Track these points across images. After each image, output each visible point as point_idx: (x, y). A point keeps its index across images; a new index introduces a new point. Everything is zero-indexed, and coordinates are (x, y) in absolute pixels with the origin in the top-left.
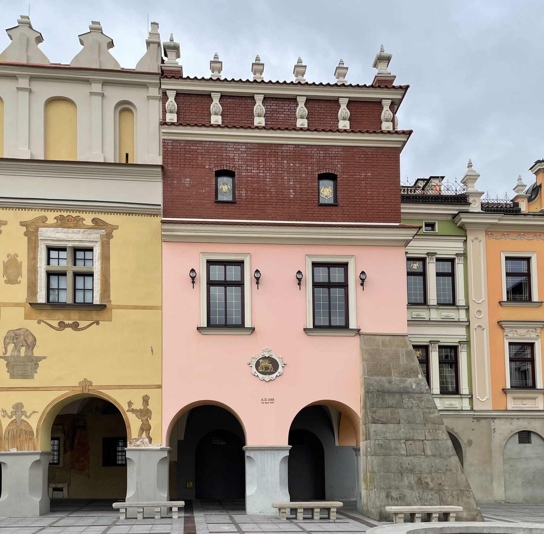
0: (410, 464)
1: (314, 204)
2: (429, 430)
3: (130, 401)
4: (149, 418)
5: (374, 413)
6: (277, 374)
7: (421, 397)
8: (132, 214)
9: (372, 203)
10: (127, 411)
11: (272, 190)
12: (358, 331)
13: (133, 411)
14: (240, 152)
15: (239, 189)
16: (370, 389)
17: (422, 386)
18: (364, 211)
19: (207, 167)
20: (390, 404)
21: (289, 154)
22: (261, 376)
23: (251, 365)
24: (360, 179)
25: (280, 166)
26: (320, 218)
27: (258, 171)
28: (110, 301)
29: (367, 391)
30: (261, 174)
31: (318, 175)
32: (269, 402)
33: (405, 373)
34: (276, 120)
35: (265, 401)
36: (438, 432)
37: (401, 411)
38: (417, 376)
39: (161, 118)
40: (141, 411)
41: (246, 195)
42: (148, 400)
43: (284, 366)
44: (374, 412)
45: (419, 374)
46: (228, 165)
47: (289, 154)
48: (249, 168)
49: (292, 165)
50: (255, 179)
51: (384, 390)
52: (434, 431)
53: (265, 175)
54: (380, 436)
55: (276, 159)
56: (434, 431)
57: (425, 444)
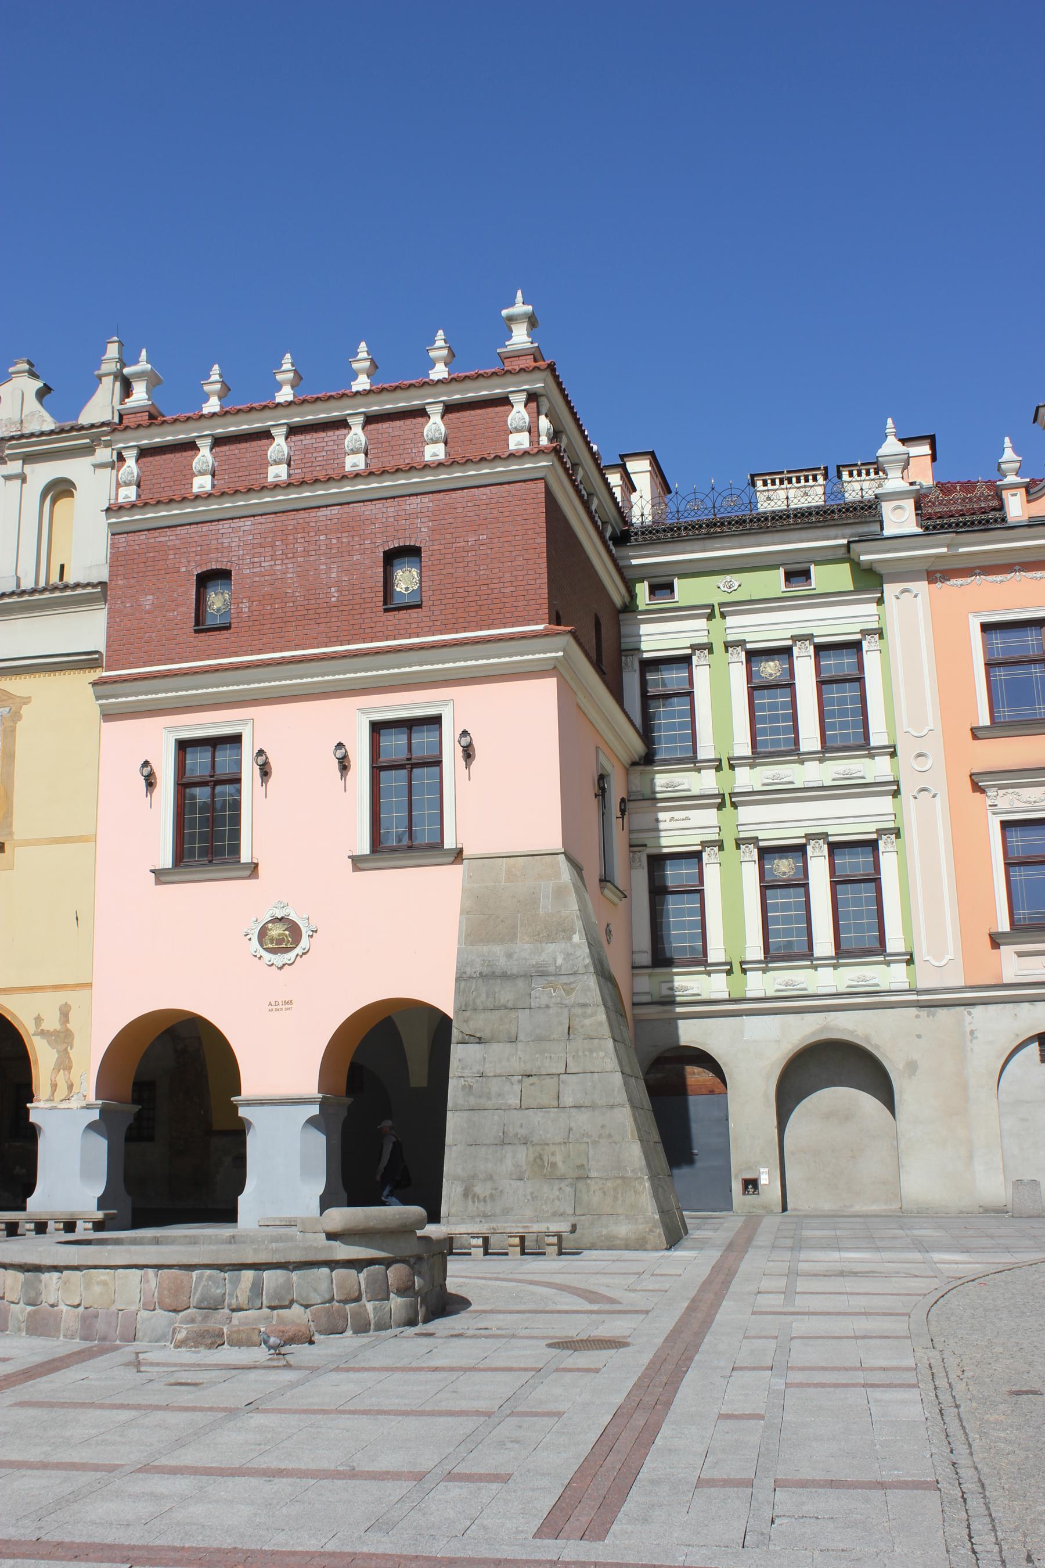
0: (524, 1125)
1: (375, 610)
2: (577, 1051)
3: (39, 1015)
4: (69, 1048)
5: (465, 1021)
6: (298, 950)
7: (570, 983)
9: (490, 592)
10: (33, 1035)
11: (297, 594)
12: (458, 855)
13: (43, 1033)
14: (241, 534)
15: (236, 601)
16: (465, 973)
17: (577, 958)
18: (473, 609)
19: (184, 569)
20: (503, 1002)
21: (329, 523)
22: (267, 956)
24: (467, 549)
25: (312, 547)
26: (386, 634)
27: (272, 563)
28: (11, 834)
29: (458, 976)
30: (279, 567)
31: (385, 553)
32: (284, 1007)
33: (545, 934)
34: (310, 464)
35: (274, 1006)
36: (595, 1054)
37: (523, 1015)
38: (570, 938)
39: (113, 496)
40: (55, 1033)
41: (249, 609)
42: (69, 1012)
44: (466, 1021)
45: (575, 933)
46: (219, 559)
47: (329, 523)
48: (256, 560)
49: (334, 541)
50: (266, 578)
51: (493, 973)
52: (587, 1053)
53: (284, 567)
54: (471, 1069)
55: (306, 535)
56: (587, 1053)
57: (562, 1082)
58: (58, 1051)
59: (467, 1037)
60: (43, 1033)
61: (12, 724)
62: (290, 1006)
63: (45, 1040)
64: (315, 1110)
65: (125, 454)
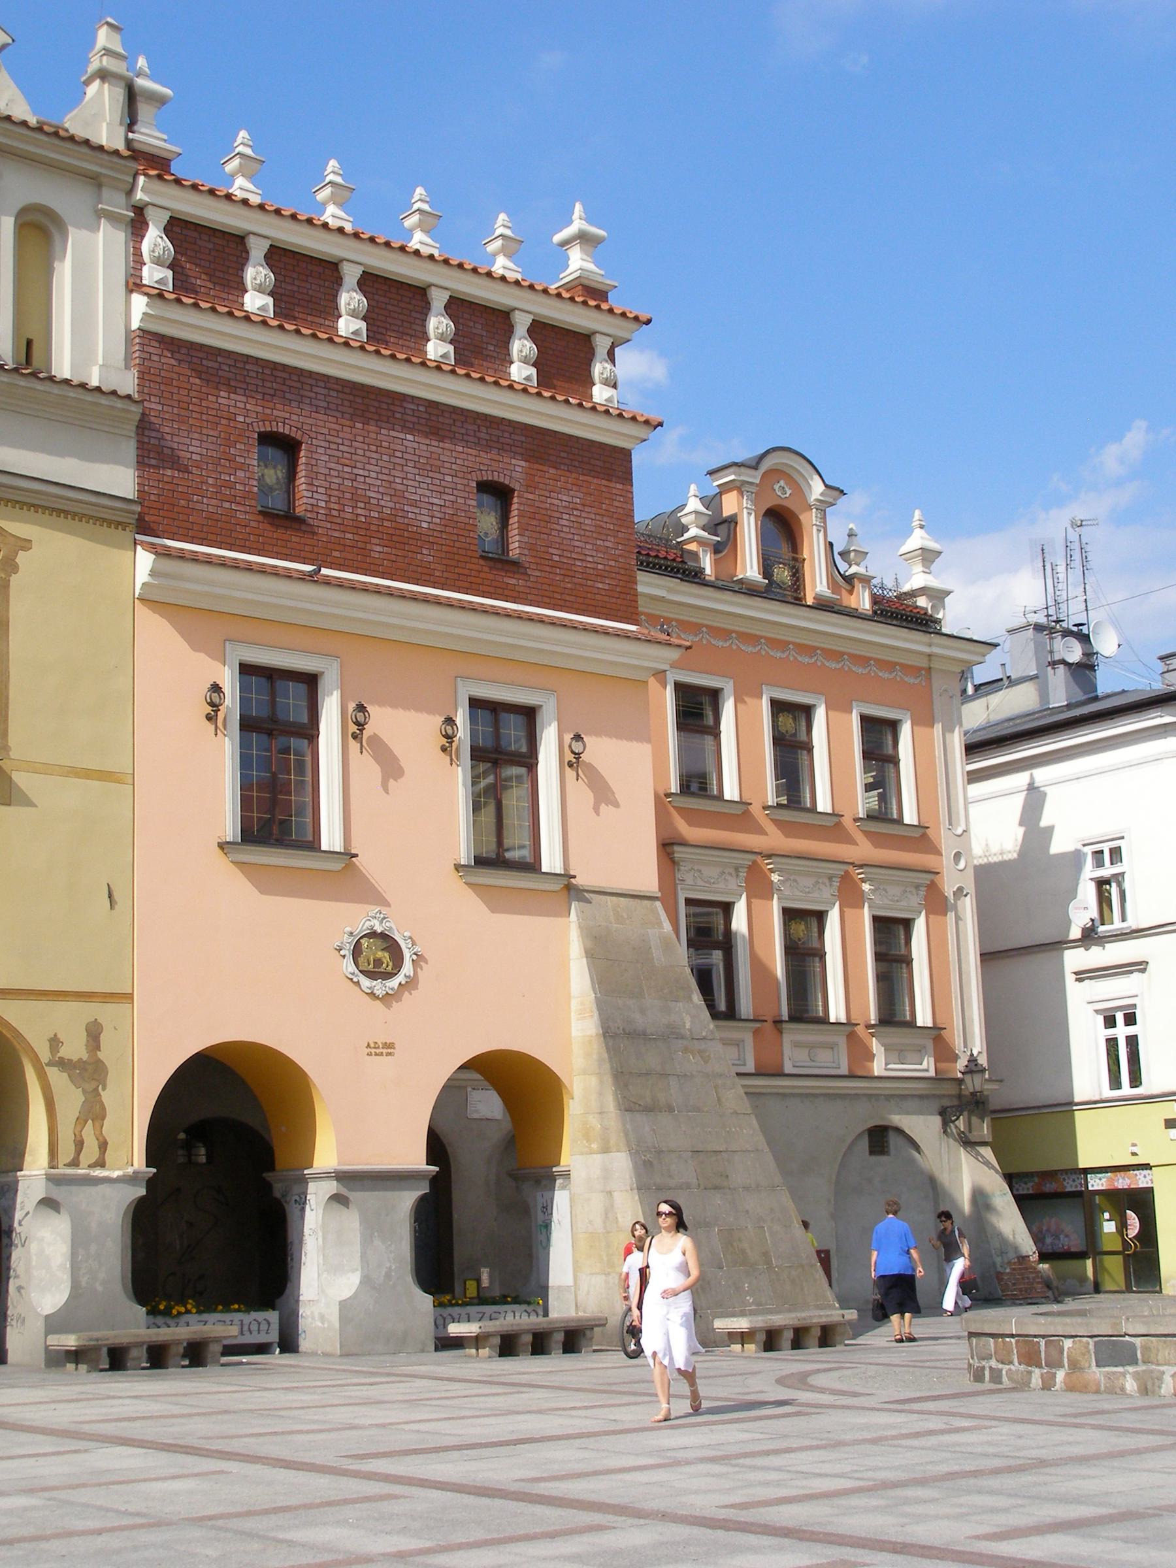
3: (55, 1035)
4: (100, 1087)
6: (400, 978)
8: (67, 513)
10: (47, 1065)
13: (63, 1064)
22: (366, 982)
23: (342, 952)
32: (385, 1051)
43: (415, 957)
58: (84, 1091)
59: (632, 1105)
60: (63, 1064)
61: (3, 576)
62: (392, 1050)
63: (65, 1075)
64: (424, 1189)
65: (150, 213)
